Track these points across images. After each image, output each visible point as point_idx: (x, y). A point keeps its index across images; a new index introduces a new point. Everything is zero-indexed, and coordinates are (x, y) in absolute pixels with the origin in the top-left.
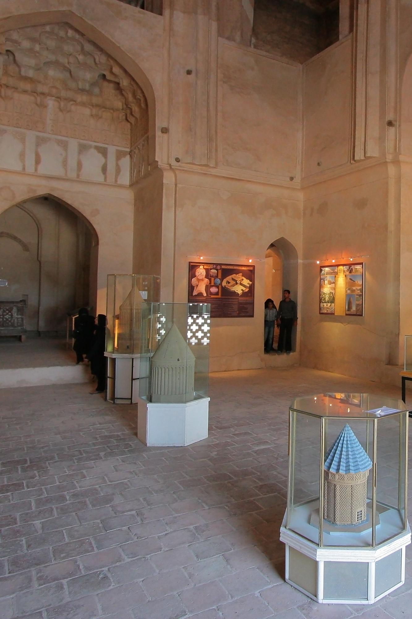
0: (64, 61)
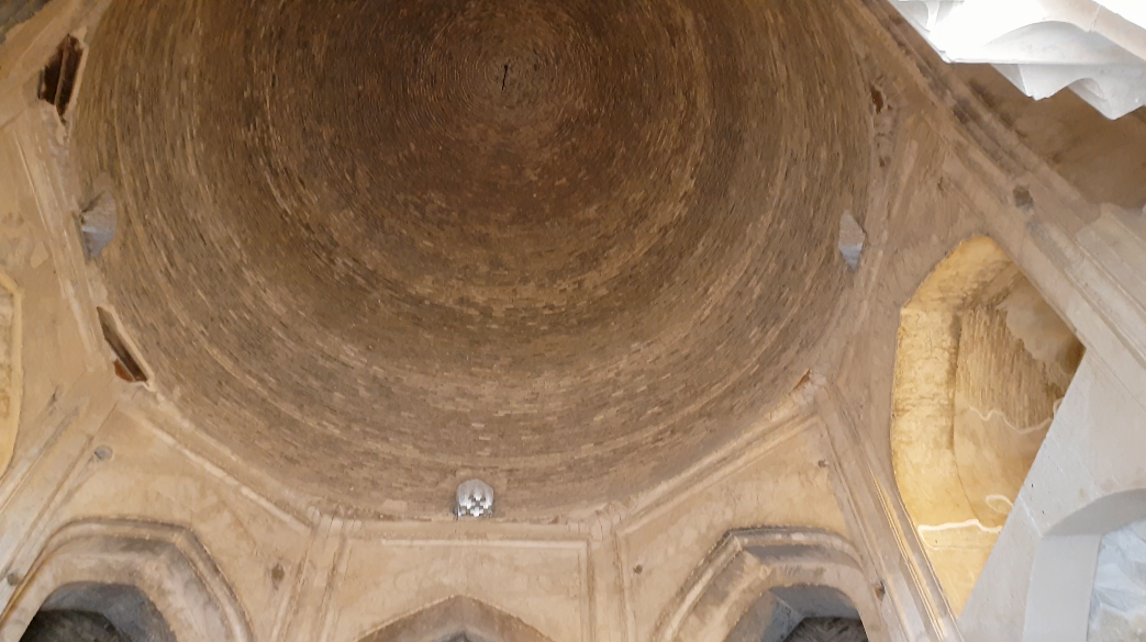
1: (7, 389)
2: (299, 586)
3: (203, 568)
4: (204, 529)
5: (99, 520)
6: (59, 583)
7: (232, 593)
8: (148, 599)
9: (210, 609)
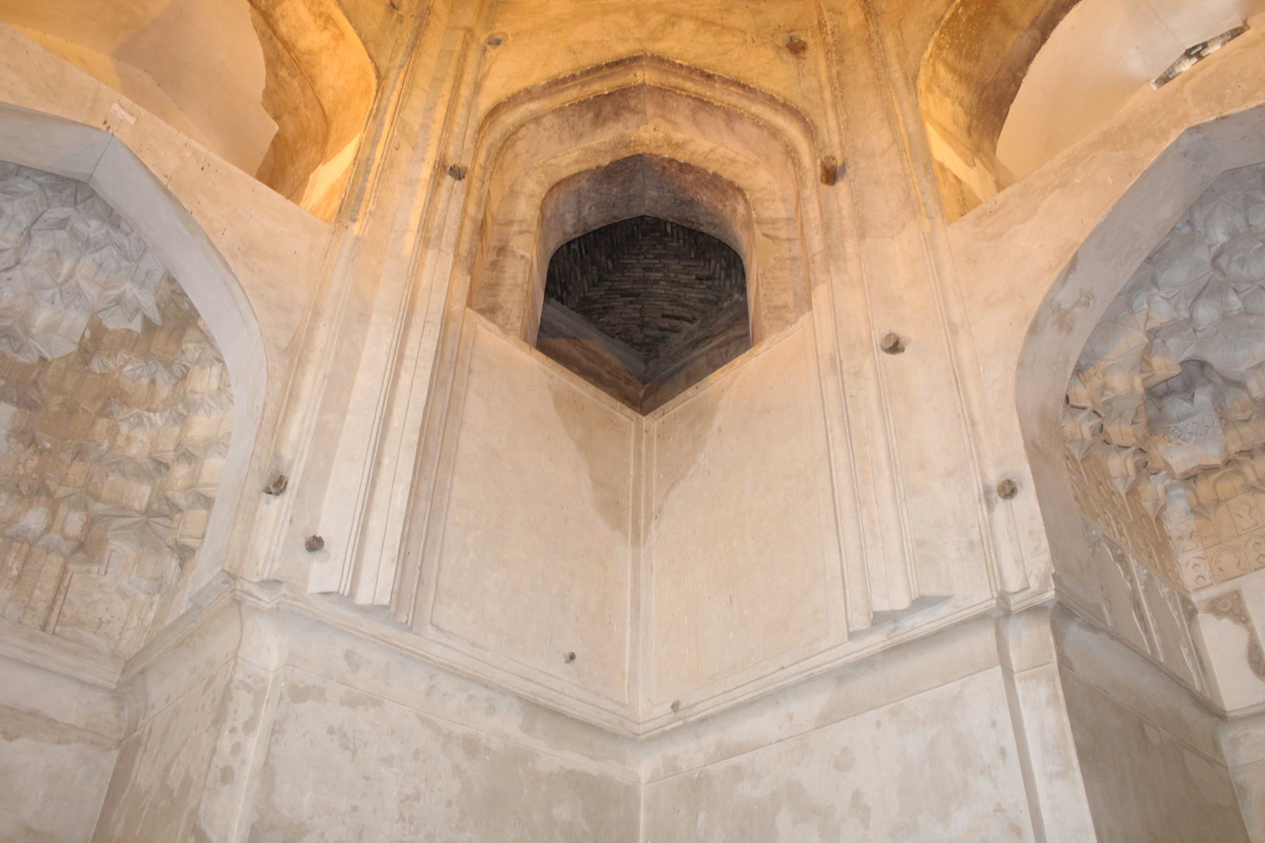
1: (322, 9)
2: (830, 39)
3: (699, 89)
4: (660, 47)
5: (529, 94)
6: (547, 186)
7: (743, 87)
8: (664, 159)
9: (737, 126)
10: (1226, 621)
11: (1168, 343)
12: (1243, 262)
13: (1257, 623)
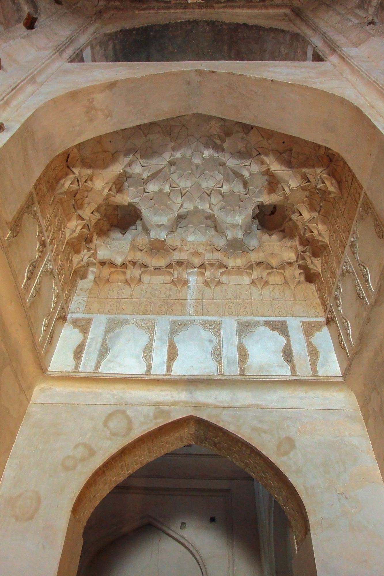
0: (203, 206)
10: (77, 330)
11: (130, 189)
12: (180, 176)
13: (90, 335)
